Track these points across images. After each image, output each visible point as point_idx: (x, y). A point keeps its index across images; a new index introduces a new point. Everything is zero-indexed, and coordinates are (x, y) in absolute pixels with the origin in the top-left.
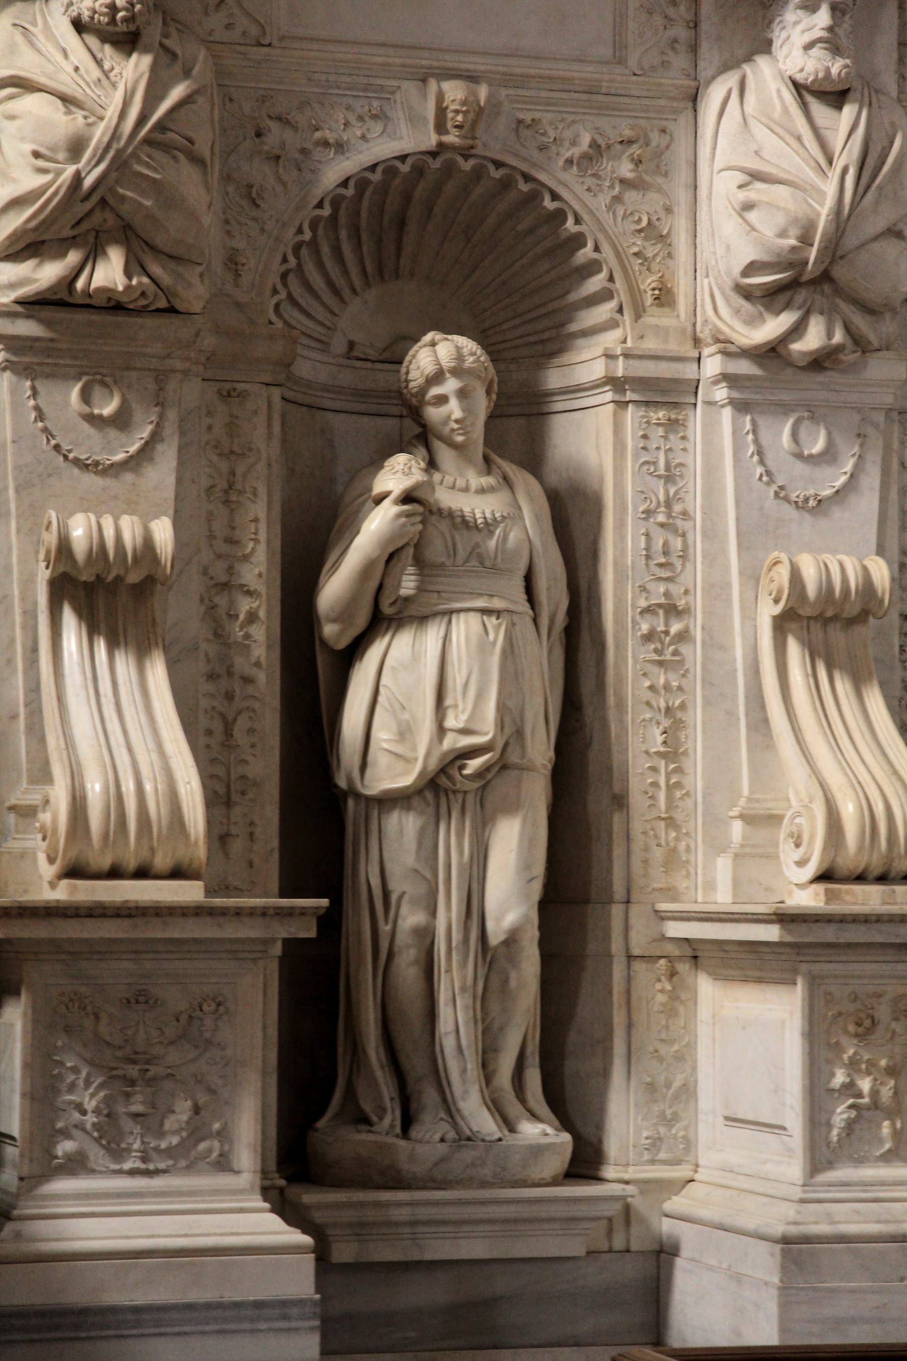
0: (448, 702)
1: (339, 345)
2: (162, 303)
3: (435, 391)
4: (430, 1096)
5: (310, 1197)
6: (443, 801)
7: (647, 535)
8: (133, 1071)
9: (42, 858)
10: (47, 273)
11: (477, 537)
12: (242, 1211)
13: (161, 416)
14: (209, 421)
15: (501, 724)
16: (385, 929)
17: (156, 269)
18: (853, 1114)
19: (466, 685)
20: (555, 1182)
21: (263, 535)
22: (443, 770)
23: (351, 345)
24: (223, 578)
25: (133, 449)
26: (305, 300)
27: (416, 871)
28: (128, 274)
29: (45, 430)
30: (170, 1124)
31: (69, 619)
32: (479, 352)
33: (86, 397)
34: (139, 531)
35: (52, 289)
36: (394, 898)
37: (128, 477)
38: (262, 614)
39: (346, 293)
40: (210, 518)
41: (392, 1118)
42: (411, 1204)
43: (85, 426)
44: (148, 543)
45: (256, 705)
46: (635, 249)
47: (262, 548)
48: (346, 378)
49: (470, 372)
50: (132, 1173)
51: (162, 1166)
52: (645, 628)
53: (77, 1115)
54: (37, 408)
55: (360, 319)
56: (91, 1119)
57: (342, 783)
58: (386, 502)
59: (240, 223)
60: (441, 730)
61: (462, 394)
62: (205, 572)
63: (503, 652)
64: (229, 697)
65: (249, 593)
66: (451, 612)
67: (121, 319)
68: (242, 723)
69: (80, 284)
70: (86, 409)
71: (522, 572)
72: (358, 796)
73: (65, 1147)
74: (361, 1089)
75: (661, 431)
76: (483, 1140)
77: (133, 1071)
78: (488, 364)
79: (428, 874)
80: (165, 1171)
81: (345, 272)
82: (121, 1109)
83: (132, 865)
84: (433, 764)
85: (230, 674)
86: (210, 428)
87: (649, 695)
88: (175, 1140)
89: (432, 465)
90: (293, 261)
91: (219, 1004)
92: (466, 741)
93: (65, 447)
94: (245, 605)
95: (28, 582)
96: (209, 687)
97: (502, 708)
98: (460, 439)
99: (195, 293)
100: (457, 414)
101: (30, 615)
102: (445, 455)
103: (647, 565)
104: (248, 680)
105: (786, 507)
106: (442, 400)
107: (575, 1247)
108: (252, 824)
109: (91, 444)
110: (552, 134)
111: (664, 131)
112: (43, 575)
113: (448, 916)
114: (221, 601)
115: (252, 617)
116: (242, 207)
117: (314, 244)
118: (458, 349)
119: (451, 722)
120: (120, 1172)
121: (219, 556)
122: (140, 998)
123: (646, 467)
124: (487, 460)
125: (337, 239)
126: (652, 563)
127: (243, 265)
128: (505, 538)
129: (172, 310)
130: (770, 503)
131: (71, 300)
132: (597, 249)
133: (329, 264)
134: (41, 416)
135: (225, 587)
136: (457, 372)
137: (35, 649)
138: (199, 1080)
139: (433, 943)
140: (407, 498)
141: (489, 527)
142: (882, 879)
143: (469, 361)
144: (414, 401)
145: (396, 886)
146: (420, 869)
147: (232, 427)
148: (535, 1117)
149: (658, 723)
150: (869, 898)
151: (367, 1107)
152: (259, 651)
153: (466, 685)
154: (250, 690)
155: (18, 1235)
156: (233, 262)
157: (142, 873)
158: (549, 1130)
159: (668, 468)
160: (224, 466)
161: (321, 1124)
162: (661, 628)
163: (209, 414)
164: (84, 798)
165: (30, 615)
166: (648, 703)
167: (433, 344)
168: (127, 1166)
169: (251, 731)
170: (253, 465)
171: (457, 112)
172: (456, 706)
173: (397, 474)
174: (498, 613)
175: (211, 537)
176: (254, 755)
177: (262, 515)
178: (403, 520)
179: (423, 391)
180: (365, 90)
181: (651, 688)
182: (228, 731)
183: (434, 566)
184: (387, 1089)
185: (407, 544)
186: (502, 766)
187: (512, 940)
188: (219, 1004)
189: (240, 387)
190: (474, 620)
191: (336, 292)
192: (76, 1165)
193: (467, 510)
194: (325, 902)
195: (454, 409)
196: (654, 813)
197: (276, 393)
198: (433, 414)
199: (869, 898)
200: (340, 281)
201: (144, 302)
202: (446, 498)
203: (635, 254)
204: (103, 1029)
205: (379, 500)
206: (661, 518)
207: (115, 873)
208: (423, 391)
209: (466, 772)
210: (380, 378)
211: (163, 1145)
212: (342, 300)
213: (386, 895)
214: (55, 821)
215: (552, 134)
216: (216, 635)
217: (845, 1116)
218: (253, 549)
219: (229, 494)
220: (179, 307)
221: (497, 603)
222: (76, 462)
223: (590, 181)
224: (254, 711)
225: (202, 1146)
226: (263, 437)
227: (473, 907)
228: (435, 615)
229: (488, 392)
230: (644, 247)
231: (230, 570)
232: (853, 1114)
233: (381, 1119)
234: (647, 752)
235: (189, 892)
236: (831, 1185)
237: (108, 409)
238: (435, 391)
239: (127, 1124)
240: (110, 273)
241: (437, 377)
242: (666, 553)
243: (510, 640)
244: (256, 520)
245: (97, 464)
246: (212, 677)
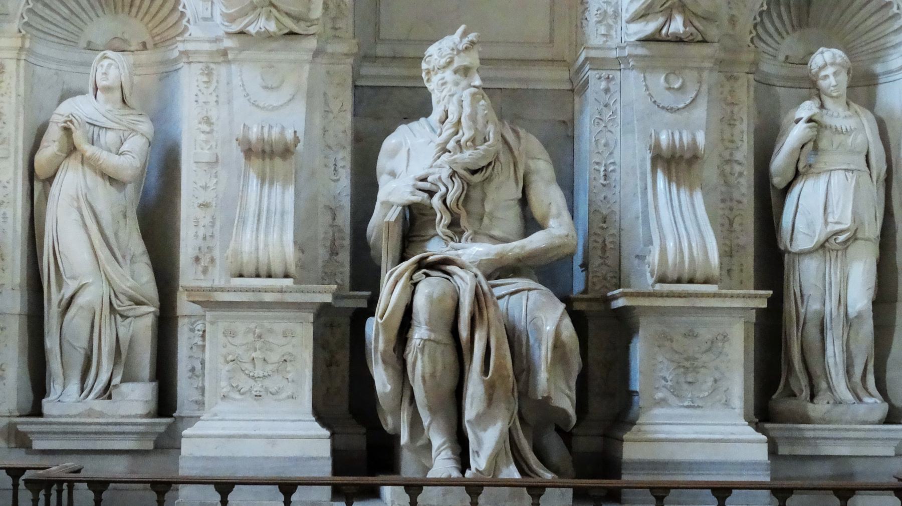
0: (829, 210)
1: (781, 58)
2: (700, 38)
3: (823, 73)
4: (824, 385)
5: (768, 426)
6: (828, 254)
8: (687, 364)
9: (648, 275)
10: (649, 27)
11: (842, 137)
13: (700, 87)
14: (721, 89)
15: (854, 221)
16: (802, 311)
17: (697, 24)
19: (838, 202)
20: (879, 423)
21: (745, 137)
22: (827, 240)
23: (787, 57)
24: (728, 157)
25: (688, 102)
26: (765, 37)
28: (685, 26)
29: (650, 94)
30: (705, 387)
31: (660, 175)
32: (843, 55)
33: (667, 80)
34: (690, 136)
35: (653, 34)
36: (805, 298)
37: (685, 114)
38: (745, 173)
39: (784, 34)
40: (722, 132)
41: (806, 393)
42: (814, 430)
43: (667, 92)
44: (694, 140)
45: (742, 213)
47: (745, 144)
48: (784, 72)
49: (839, 64)
50: (688, 407)
53: (663, 382)
54: (646, 86)
55: (790, 45)
56: (670, 383)
57: (782, 248)
58: (800, 122)
60: (826, 223)
61: (835, 74)
62: (720, 155)
63: (855, 187)
64: (731, 209)
65: (740, 164)
66: (831, 171)
67: (682, 45)
68: (737, 220)
69: (664, 31)
70: (667, 86)
71: (865, 153)
72: (789, 252)
73: (659, 395)
74: (792, 382)
77: (687, 364)
78: (848, 60)
79: (821, 287)
81: (783, 22)
82: (682, 380)
83: (686, 276)
84: (823, 239)
85: (731, 200)
86: (722, 93)
88: (706, 394)
89: (822, 106)
90: (759, 19)
91: (725, 337)
92: (838, 227)
93: (658, 101)
94: (737, 168)
95: (644, 159)
96: (722, 205)
97: (854, 213)
98: (835, 94)
99: (713, 32)
100: (834, 83)
101: (644, 174)
102: (828, 102)
104: (739, 202)
106: (826, 77)
107: (891, 452)
108: (742, 265)
109: (668, 99)
112: (649, 156)
113: (831, 306)
114: (727, 168)
115: (741, 174)
117: (769, 11)
118: (834, 55)
119: (830, 219)
120: (681, 407)
121: (727, 149)
122: (691, 334)
124: (848, 104)
125: (780, 11)
128: (855, 139)
129: (704, 41)
131: (660, 38)
132: (898, 8)
133: (777, 21)
134: (647, 89)
135: (728, 162)
136: (832, 64)
137: (646, 189)
138: (717, 369)
139: (823, 319)
140: (810, 120)
141: (848, 132)
143: (839, 60)
144: (814, 79)
147: (732, 92)
148: (871, 395)
151: (796, 391)
152: (744, 190)
153: (838, 202)
154: (740, 206)
155: (639, 431)
156: (733, 20)
157: (691, 281)
158: (878, 401)
160: (728, 109)
161: (774, 397)
163: (722, 86)
164: (666, 249)
165: (644, 174)
167: (822, 53)
168: (686, 404)
169: (741, 224)
172: (833, 212)
173: (807, 109)
174: (853, 171)
175: (723, 140)
177: (745, 129)
179: (817, 73)
182: (731, 224)
183: (823, 150)
184: (804, 382)
185: (810, 140)
186: (854, 238)
187: (859, 316)
188: (725, 337)
189: (735, 74)
190: (841, 174)
191: (780, 34)
192: (662, 403)
193: (838, 126)
194: (771, 292)
195: (832, 81)
197: (751, 76)
198: (823, 84)
200: (781, 29)
201: (691, 38)
202: (827, 120)
204: (675, 346)
205: (797, 121)
207: (679, 281)
208: (817, 73)
210: (799, 71)
211: (701, 396)
212: (783, 38)
213: (802, 296)
214: (653, 259)
216: (725, 182)
219: (730, 121)
220: (707, 39)
221: (852, 167)
222: (663, 108)
225: (718, 397)
226: (745, 95)
227: (842, 301)
228: (825, 171)
229: (848, 73)
231: (731, 155)
233: (801, 394)
237: (676, 86)
238: (823, 73)
239: (685, 386)
240: (677, 25)
241: (825, 66)
243: (857, 183)
244: (742, 132)
245: (672, 109)
246: (723, 201)
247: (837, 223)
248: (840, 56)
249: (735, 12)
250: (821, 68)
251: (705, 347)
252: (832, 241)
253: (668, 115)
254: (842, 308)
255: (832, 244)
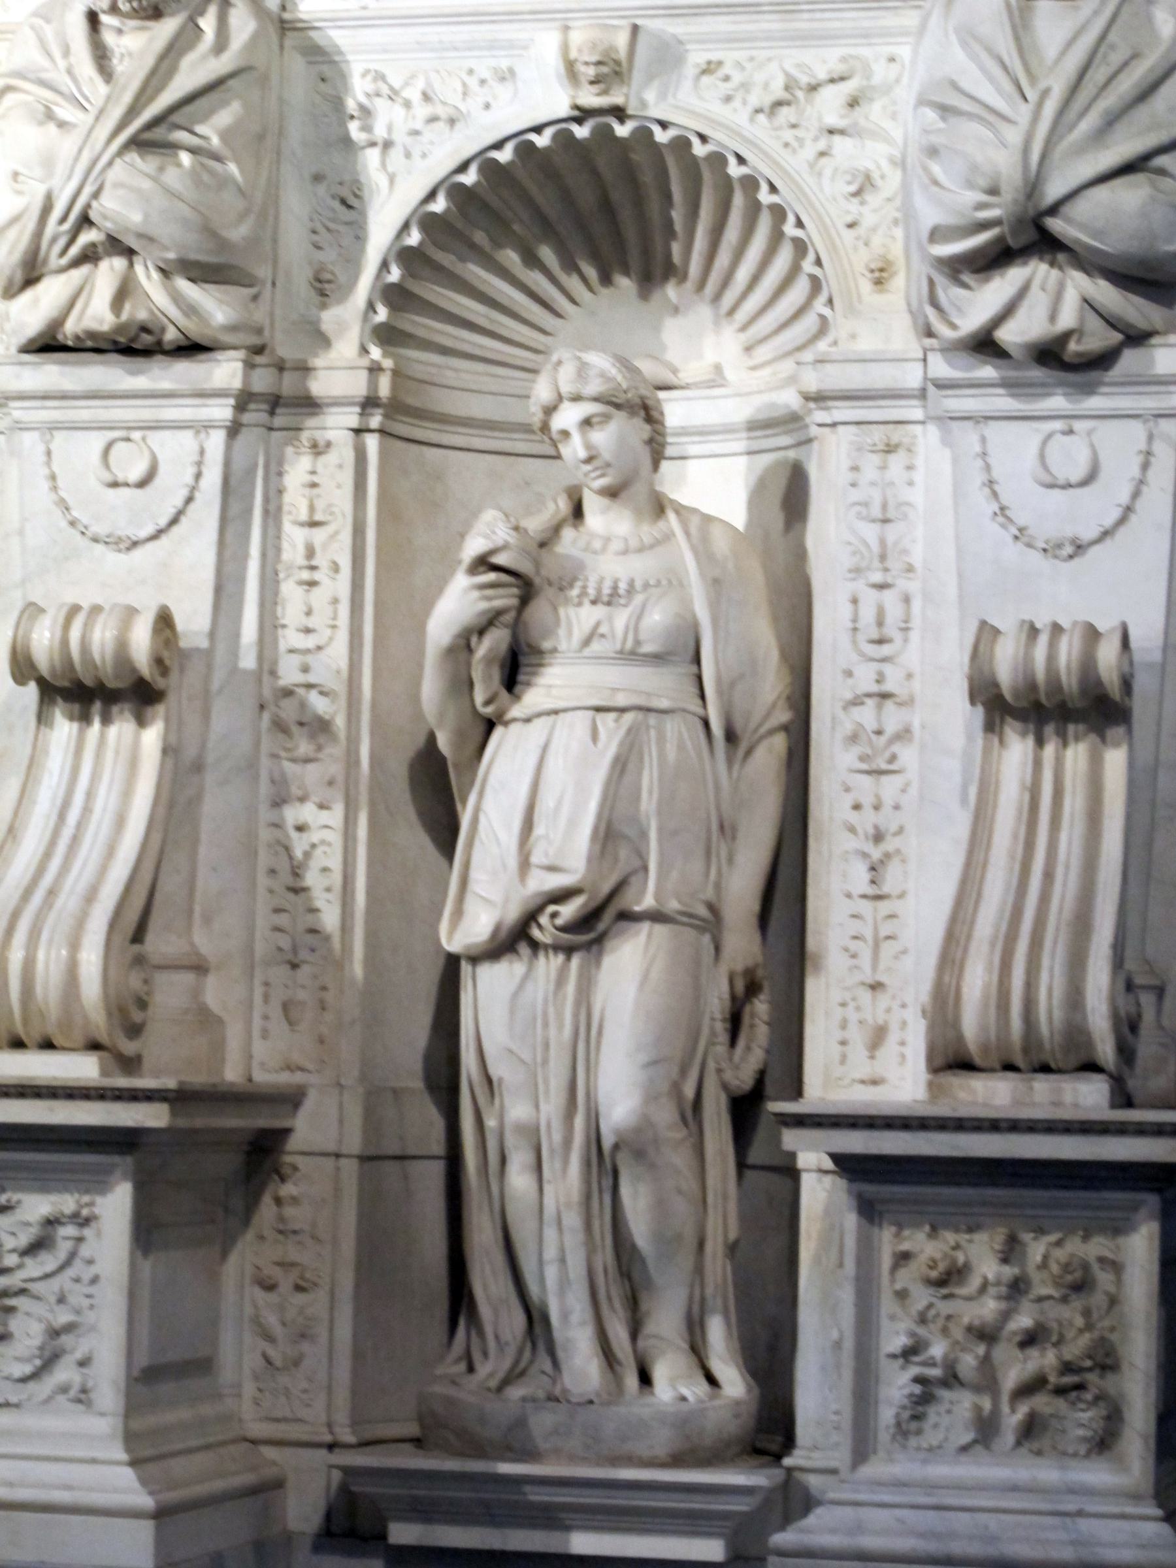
7: (855, 601)
12: (94, 1461)
16: (491, 1123)
18: (917, 1389)
27: (511, 1051)
36: (495, 1084)
46: (849, 219)
51: (13, 1399)
52: (848, 727)
59: (328, 230)
60: (525, 865)
70: (108, 478)
75: (876, 459)
76: (569, 1402)
80: (17, 1406)
84: (513, 914)
87: (853, 817)
103: (854, 642)
105: (1035, 557)
108: (324, 988)
110: (737, 77)
111: (892, 60)
113: (551, 1108)
116: (333, 210)
123: (858, 508)
126: (861, 638)
127: (329, 282)
130: (1013, 552)
134: (55, 488)
136: (577, 398)
142: (1009, 1067)
145: (497, 1070)
146: (514, 1048)
149: (865, 855)
150: (992, 1094)
159: (884, 506)
162: (870, 724)
166: (852, 830)
170: (337, 533)
171: (587, 63)
176: (329, 901)
178: (476, 594)
180: (491, 48)
181: (857, 807)
196: (858, 977)
199: (992, 1094)
201: (147, 339)
203: (851, 226)
206: (877, 577)
209: (559, 921)
215: (737, 77)
217: (906, 1391)
218: (331, 639)
223: (788, 135)
224: (329, 844)
230: (861, 214)
232: (917, 1389)
234: (849, 896)
235: (83, 1068)
236: (880, 1484)
242: (880, 623)
244: (335, 601)
247: (552, 869)
248: (602, 375)
249: (328, 256)
250: (550, 410)
251: (24, 1240)
252: (544, 920)
253: (113, 560)
254: (579, 1122)
255: (544, 932)
